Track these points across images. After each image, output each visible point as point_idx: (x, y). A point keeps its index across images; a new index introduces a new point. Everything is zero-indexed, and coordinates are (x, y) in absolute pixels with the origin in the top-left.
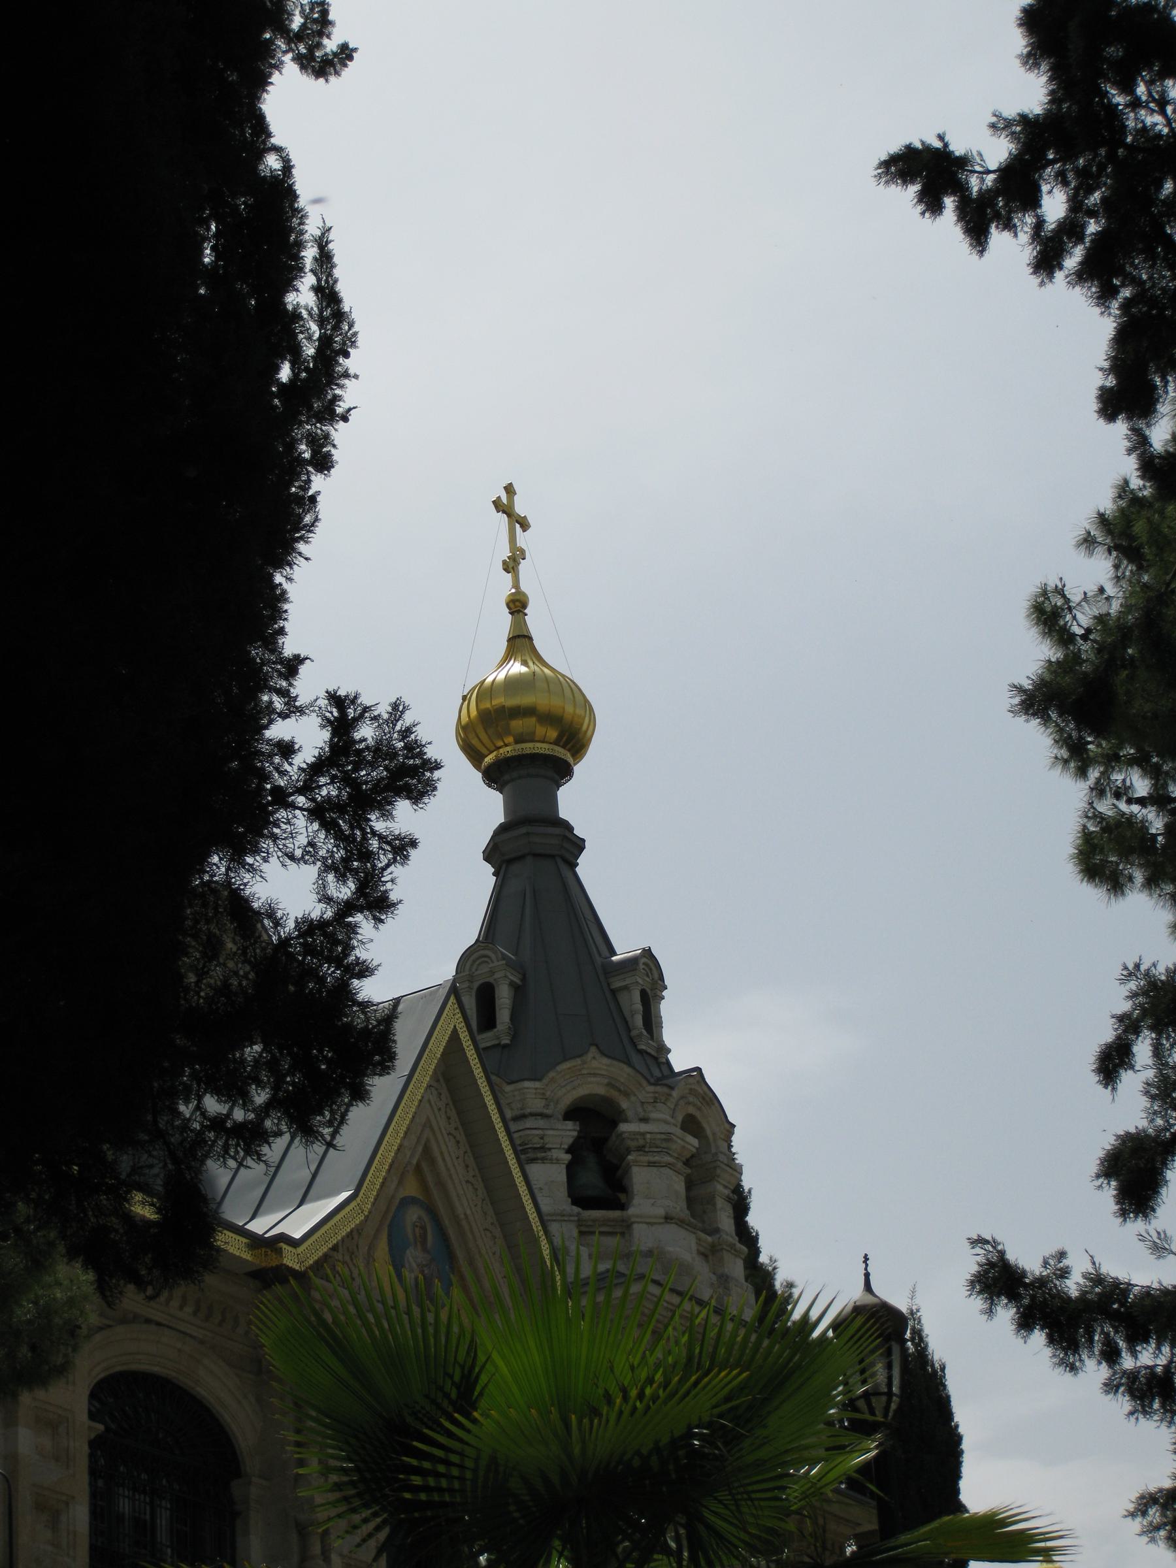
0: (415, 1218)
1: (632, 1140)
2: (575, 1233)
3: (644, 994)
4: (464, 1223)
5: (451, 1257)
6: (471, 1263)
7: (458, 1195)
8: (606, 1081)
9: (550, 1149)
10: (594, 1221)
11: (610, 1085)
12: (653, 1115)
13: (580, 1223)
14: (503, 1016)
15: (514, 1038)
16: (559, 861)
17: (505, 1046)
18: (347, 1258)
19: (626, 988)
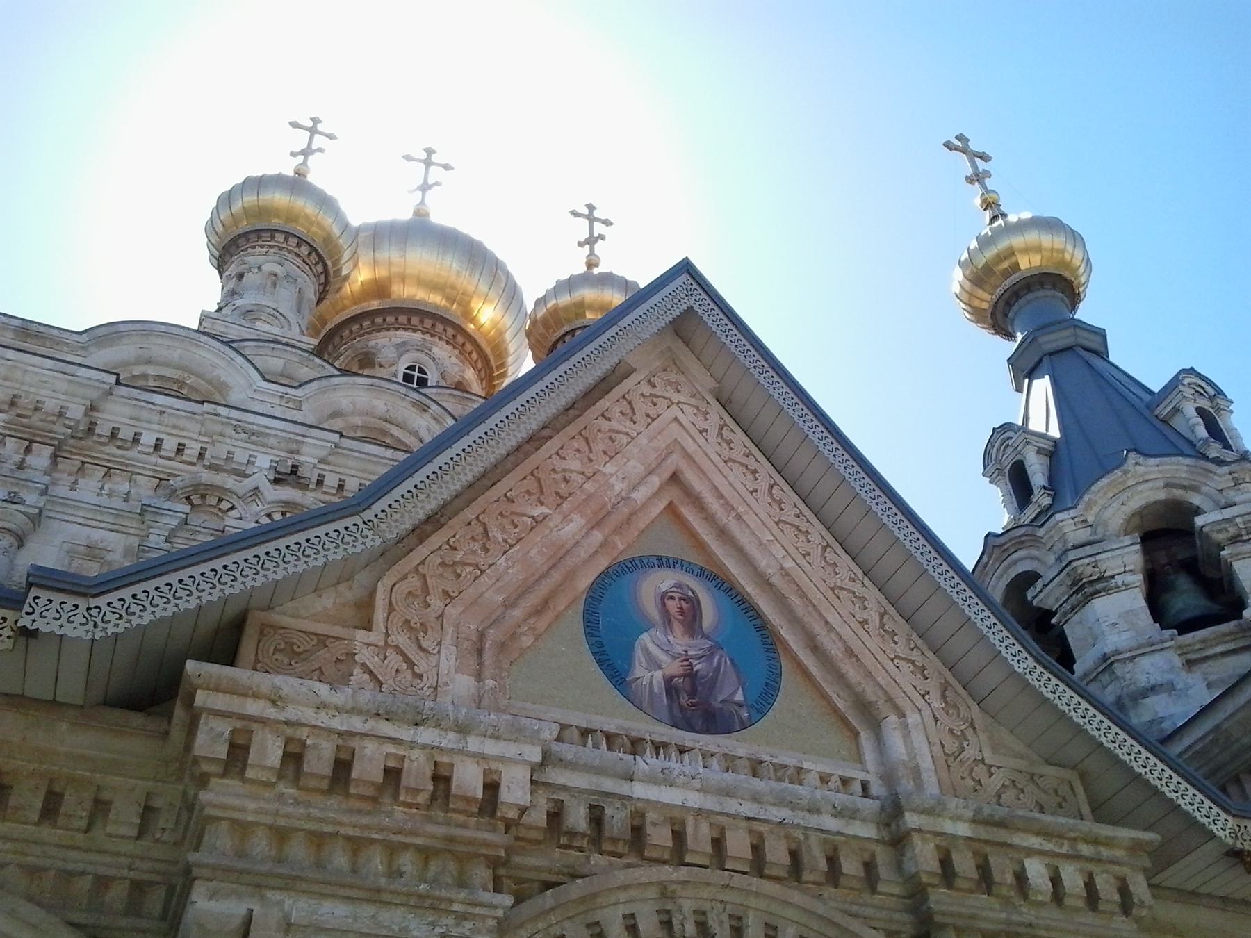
0: (664, 587)
1: (1219, 532)
2: (1178, 661)
3: (1201, 412)
5: (769, 640)
6: (815, 648)
10: (1203, 641)
11: (1167, 486)
12: (1237, 499)
13: (1182, 651)
14: (1038, 478)
15: (1054, 497)
17: (1050, 507)
18: (403, 640)
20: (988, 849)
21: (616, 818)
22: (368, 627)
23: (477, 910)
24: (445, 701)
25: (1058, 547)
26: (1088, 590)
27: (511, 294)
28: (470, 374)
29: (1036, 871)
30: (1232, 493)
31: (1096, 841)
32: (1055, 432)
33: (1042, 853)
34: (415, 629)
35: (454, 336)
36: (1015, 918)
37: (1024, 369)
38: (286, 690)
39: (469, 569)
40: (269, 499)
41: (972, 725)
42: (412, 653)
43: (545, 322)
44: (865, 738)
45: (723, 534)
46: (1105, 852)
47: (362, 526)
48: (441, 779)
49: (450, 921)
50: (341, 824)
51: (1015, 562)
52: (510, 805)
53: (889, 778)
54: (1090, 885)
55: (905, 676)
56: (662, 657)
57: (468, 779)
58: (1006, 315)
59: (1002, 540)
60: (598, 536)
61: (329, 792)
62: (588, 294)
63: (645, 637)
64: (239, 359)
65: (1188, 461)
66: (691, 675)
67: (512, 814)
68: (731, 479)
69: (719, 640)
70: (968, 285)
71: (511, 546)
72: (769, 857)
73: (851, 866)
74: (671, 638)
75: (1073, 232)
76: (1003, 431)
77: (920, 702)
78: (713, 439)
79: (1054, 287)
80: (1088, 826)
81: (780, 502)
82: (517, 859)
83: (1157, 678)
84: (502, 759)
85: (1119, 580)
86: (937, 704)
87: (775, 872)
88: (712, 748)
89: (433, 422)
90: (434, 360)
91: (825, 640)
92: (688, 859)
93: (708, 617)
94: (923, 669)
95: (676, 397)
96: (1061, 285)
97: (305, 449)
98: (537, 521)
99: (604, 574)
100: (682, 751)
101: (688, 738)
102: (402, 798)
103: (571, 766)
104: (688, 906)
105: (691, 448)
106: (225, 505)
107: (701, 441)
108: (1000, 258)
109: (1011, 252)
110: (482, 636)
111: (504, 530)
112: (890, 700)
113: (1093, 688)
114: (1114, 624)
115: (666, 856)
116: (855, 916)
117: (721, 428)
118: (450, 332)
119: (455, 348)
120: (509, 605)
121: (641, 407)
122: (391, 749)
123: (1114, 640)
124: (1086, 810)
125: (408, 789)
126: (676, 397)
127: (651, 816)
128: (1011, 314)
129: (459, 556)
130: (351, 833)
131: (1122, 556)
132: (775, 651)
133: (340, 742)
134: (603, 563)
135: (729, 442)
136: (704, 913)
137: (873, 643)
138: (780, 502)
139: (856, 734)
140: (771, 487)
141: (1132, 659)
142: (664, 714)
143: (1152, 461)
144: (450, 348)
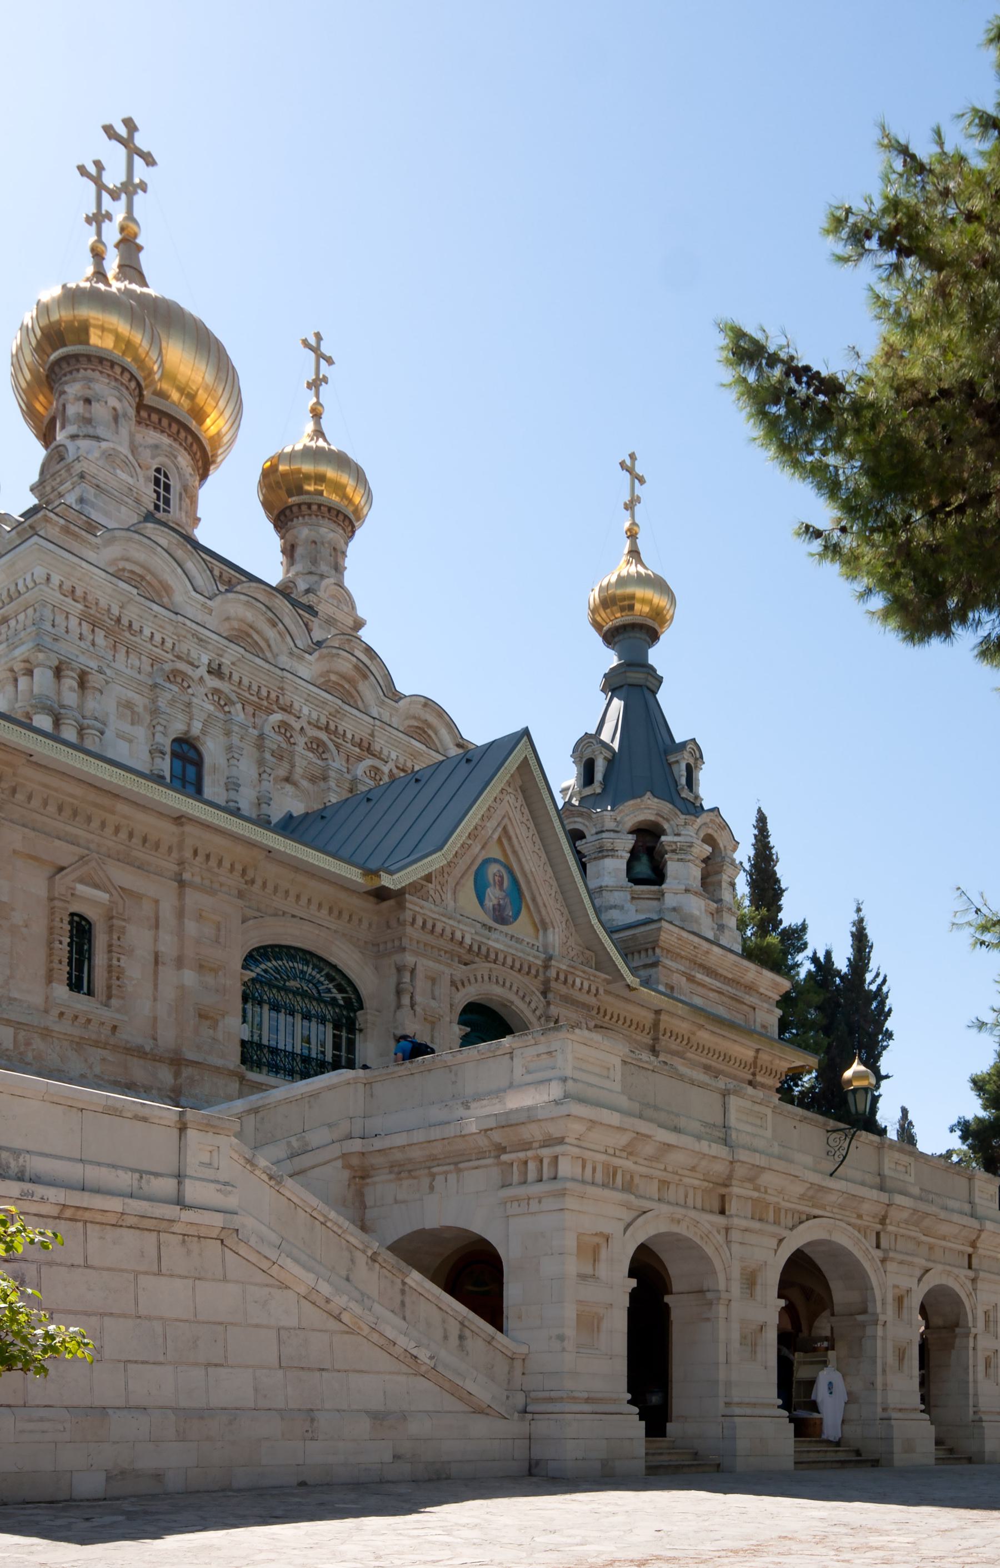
26: (605, 853)
35: (192, 444)
40: (209, 686)
64: (179, 570)
83: (618, 902)
90: (177, 468)
97: (226, 655)
106: (185, 684)
118: (190, 439)
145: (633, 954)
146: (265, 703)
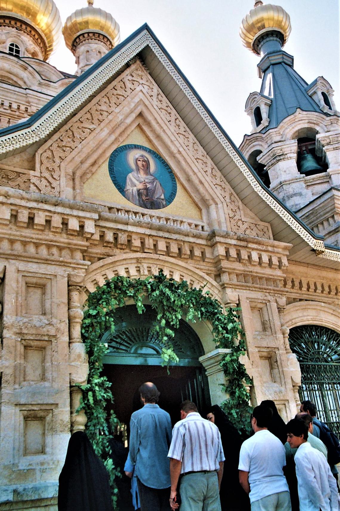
0: (137, 156)
1: (324, 140)
2: (304, 185)
3: (323, 94)
4: (178, 156)
6: (189, 180)
7: (172, 141)
8: (307, 121)
9: (286, 154)
10: (313, 179)
12: (332, 129)
13: (306, 182)
16: (283, 64)
17: (267, 126)
18: (47, 175)
19: (315, 93)
20: (240, 248)
21: (123, 238)
22: (33, 169)
23: (79, 266)
24: (63, 196)
25: (269, 142)
26: (278, 158)
27: (55, 13)
28: (38, 49)
29: (255, 256)
30: (330, 127)
31: (273, 246)
32: (272, 97)
33: (257, 249)
34: (51, 171)
36: (247, 269)
37: (263, 70)
38: (10, 193)
39: (68, 148)
41: (239, 208)
42: (51, 179)
43: (71, 29)
44: (204, 211)
45: (158, 137)
46: (276, 250)
47: (31, 133)
48: (65, 223)
49: (70, 269)
50: (32, 238)
51: (254, 146)
52: (89, 233)
53: (210, 224)
54: (270, 260)
55: (218, 191)
56: (137, 183)
57: (74, 224)
58: (258, 46)
59: (249, 138)
60: (113, 137)
61: (28, 227)
62: (90, 17)
63: (130, 175)
65: (317, 114)
66: (146, 189)
67: (89, 236)
68: (162, 116)
69: (156, 176)
70: (245, 31)
71: (83, 140)
72: (172, 250)
73: (197, 253)
74: (139, 175)
75: (286, 13)
76: (253, 95)
77: (223, 200)
78: (155, 98)
79: (277, 36)
80: (272, 241)
81: (179, 126)
82: (90, 250)
84: (85, 218)
85: (289, 155)
86: (228, 200)
87: (173, 255)
88: (153, 214)
89: (30, 75)
90: (22, 41)
91: (194, 178)
92: (146, 251)
93: (153, 167)
94: (225, 188)
95: (141, 82)
96: (280, 36)
98: (92, 131)
99: (116, 151)
100: (143, 215)
101: (145, 211)
102: (52, 230)
103: (107, 220)
104: (145, 265)
105: (147, 103)
107: (151, 100)
108: (258, 21)
109: (262, 20)
110: (74, 173)
111: (80, 134)
112: (213, 199)
113: (275, 193)
114: (285, 171)
115: (139, 250)
116: (198, 269)
117: (158, 95)
118: (29, 29)
119: (31, 36)
120: (82, 162)
121: (129, 85)
122: (48, 214)
123: (284, 177)
124: (272, 237)
125: (54, 227)
126: (141, 82)
127: (134, 236)
128: (260, 46)
129: (64, 144)
130: (35, 241)
131: (291, 147)
132: (175, 181)
133: (30, 211)
134: (114, 147)
135: (161, 101)
136: (150, 268)
137: (209, 179)
138: (179, 126)
139: (200, 210)
140: (176, 120)
141: (289, 184)
142: (137, 202)
143: (305, 113)
144: (29, 36)
145: (317, 226)
146: (17, 113)
